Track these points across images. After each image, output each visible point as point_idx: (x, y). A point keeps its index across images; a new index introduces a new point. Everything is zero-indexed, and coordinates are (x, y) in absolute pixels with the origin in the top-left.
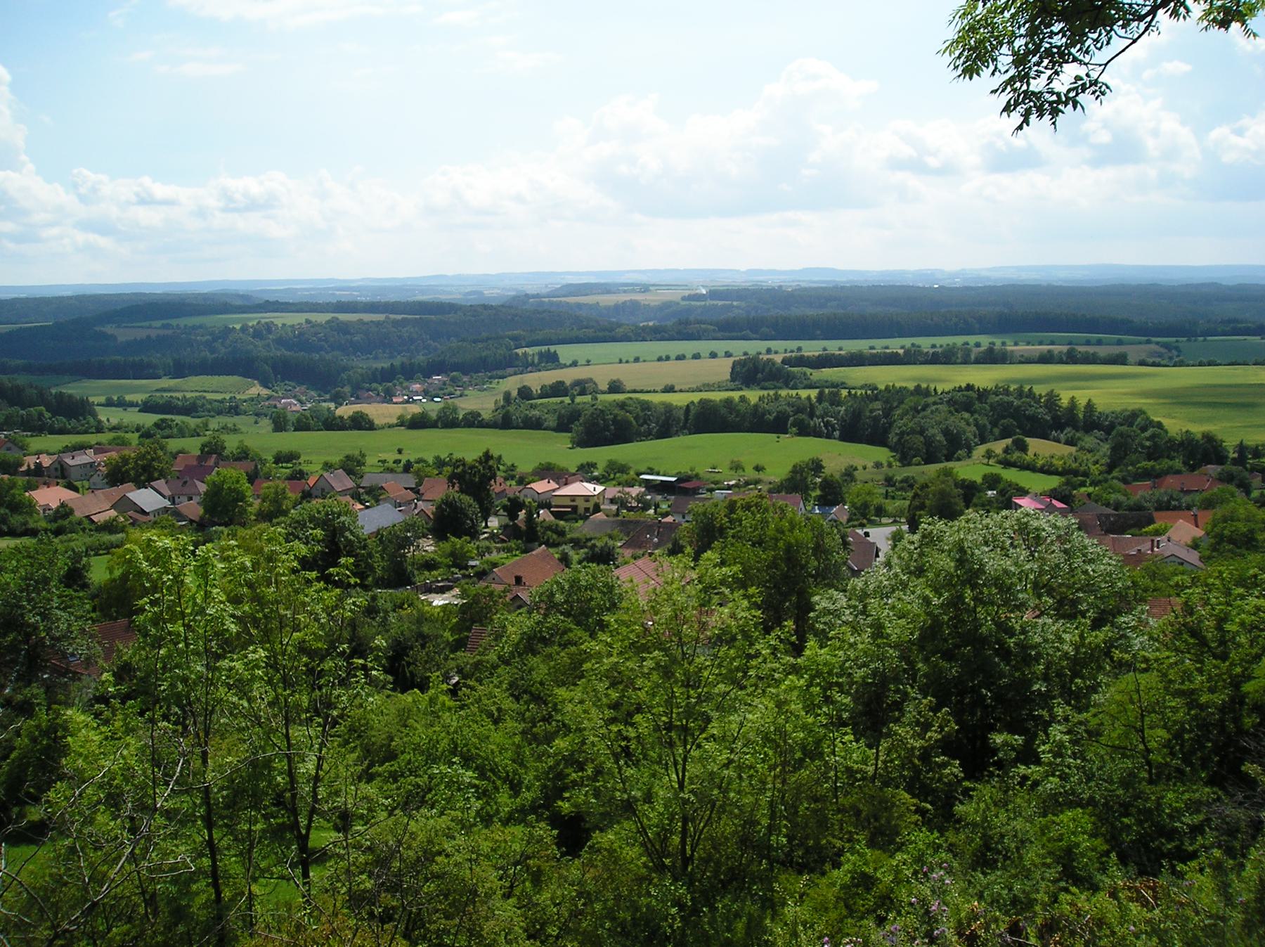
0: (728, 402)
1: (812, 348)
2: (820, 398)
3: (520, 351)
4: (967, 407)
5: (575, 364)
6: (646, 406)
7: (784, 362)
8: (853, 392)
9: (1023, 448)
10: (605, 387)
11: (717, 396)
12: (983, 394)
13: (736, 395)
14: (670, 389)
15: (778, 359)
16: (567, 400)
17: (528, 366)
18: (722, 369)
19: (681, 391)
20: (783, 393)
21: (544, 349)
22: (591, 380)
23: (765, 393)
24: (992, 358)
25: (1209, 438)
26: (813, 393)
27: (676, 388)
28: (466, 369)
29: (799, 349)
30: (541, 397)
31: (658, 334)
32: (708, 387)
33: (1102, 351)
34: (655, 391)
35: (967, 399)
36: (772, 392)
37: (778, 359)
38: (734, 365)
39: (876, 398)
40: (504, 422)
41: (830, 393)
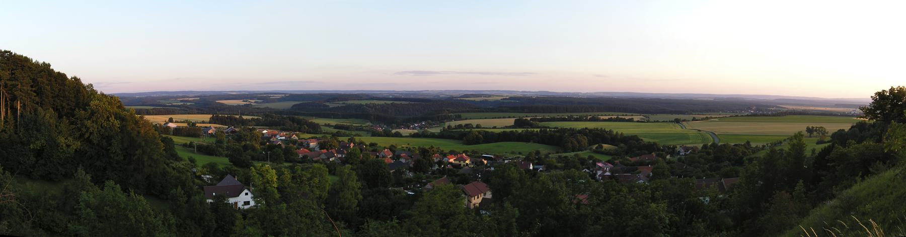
1: (540, 116)
4: (586, 134)
9: (602, 147)
11: (508, 130)
12: (591, 131)
14: (495, 128)
17: (450, 119)
18: (511, 122)
24: (594, 119)
25: (655, 144)
31: (492, 110)
32: (507, 127)
33: (627, 118)
35: (583, 132)
39: (557, 132)
40: (441, 136)
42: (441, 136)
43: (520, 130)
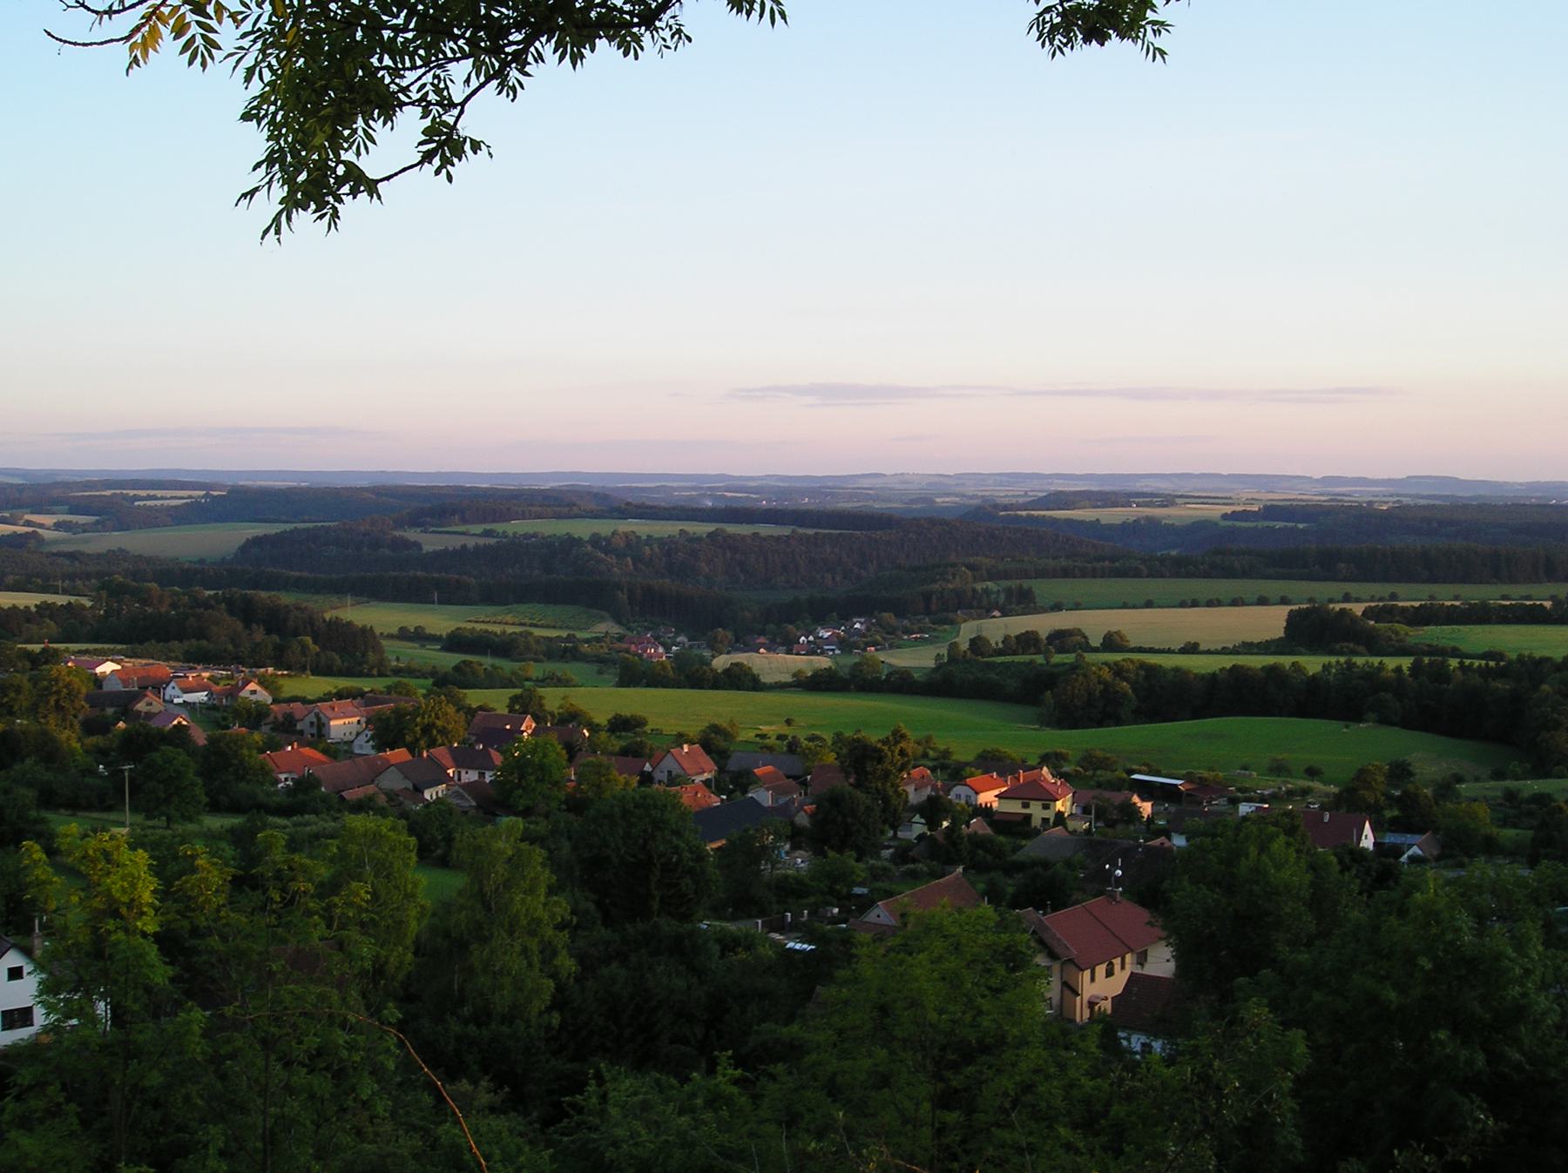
0: (1272, 670)
1: (1411, 597)
2: (1415, 669)
3: (979, 587)
5: (1057, 607)
6: (1151, 670)
7: (1367, 613)
8: (1467, 662)
10: (1096, 642)
11: (1257, 662)
13: (1286, 661)
15: (1358, 609)
16: (1040, 659)
17: (983, 607)
18: (1271, 621)
19: (1209, 652)
20: (1359, 661)
21: (1014, 584)
22: (1079, 632)
23: (1333, 659)
26: (1406, 663)
27: (1202, 648)
28: (900, 609)
29: (1394, 597)
30: (1000, 653)
31: (1181, 568)
32: (1248, 648)
34: (1170, 651)
36: (1342, 659)
37: (1358, 609)
38: (1292, 617)
39: (1501, 673)
41: (1431, 664)
42: (940, 685)
43: (1312, 664)
